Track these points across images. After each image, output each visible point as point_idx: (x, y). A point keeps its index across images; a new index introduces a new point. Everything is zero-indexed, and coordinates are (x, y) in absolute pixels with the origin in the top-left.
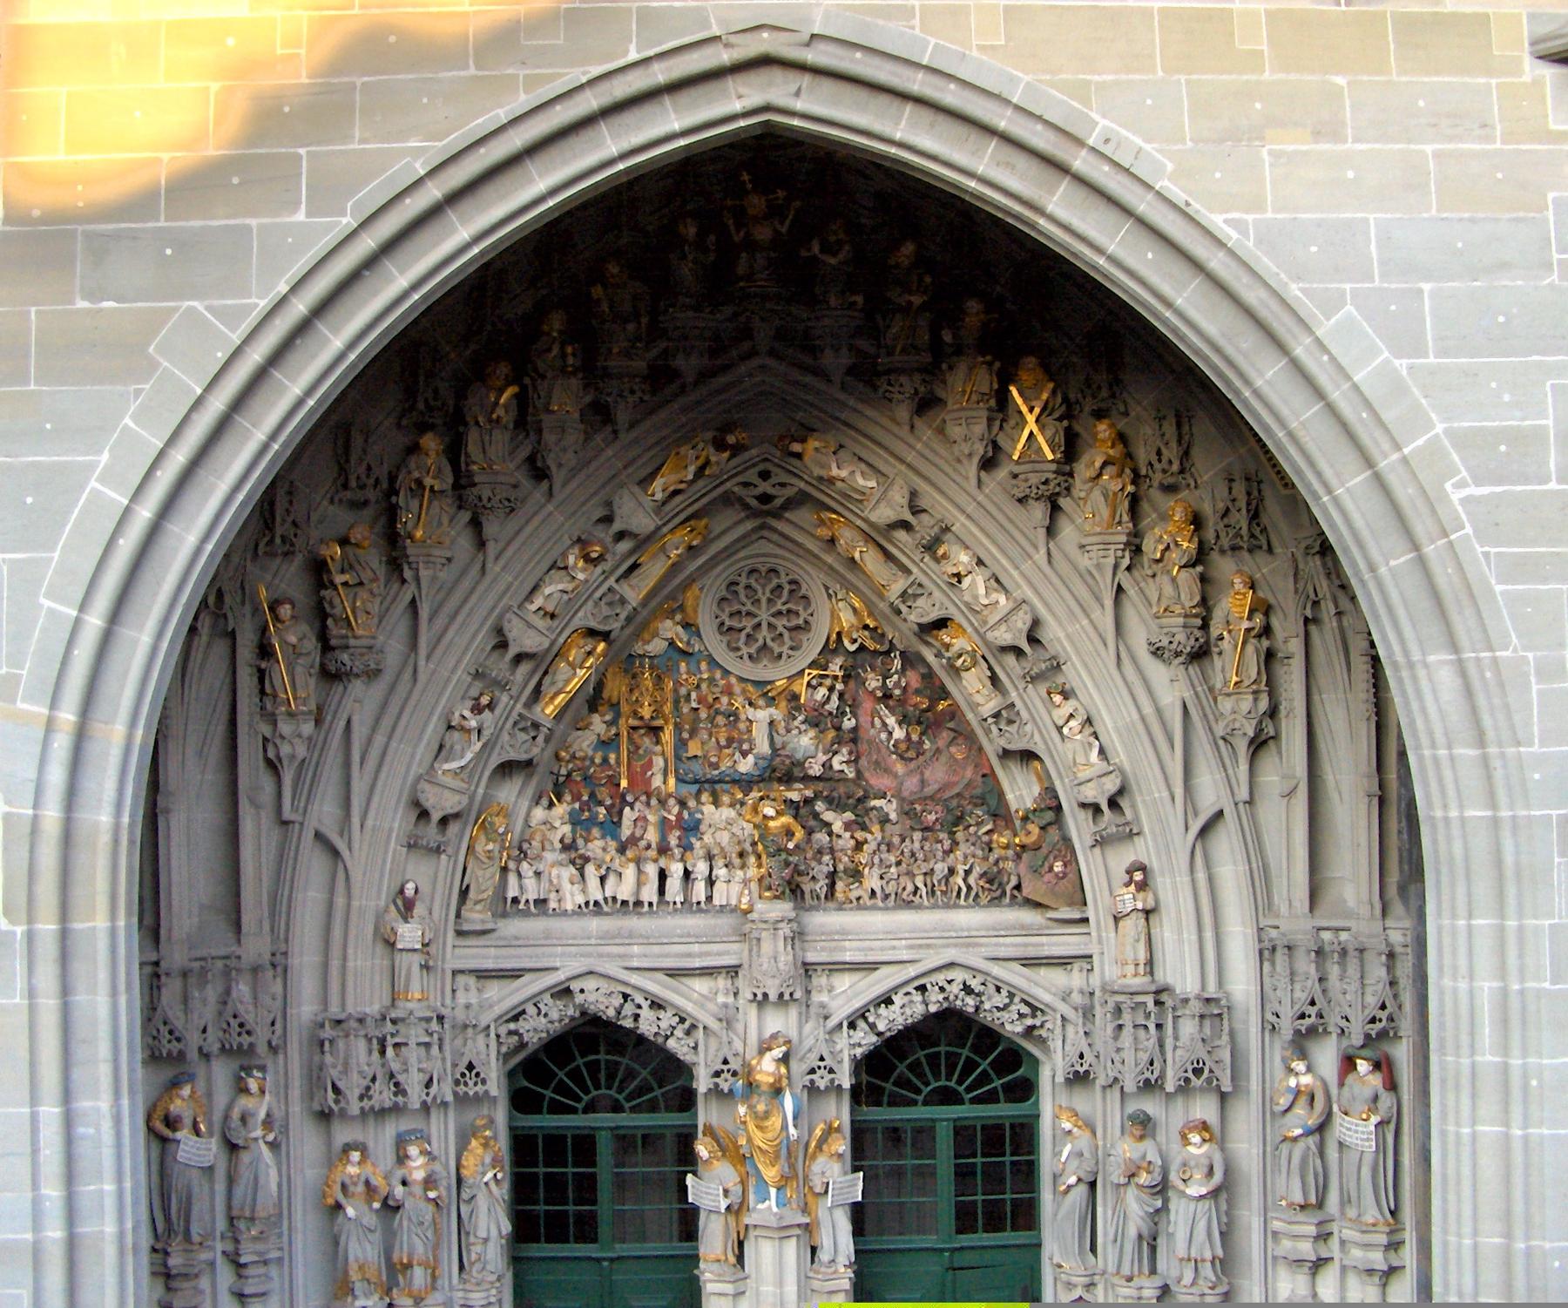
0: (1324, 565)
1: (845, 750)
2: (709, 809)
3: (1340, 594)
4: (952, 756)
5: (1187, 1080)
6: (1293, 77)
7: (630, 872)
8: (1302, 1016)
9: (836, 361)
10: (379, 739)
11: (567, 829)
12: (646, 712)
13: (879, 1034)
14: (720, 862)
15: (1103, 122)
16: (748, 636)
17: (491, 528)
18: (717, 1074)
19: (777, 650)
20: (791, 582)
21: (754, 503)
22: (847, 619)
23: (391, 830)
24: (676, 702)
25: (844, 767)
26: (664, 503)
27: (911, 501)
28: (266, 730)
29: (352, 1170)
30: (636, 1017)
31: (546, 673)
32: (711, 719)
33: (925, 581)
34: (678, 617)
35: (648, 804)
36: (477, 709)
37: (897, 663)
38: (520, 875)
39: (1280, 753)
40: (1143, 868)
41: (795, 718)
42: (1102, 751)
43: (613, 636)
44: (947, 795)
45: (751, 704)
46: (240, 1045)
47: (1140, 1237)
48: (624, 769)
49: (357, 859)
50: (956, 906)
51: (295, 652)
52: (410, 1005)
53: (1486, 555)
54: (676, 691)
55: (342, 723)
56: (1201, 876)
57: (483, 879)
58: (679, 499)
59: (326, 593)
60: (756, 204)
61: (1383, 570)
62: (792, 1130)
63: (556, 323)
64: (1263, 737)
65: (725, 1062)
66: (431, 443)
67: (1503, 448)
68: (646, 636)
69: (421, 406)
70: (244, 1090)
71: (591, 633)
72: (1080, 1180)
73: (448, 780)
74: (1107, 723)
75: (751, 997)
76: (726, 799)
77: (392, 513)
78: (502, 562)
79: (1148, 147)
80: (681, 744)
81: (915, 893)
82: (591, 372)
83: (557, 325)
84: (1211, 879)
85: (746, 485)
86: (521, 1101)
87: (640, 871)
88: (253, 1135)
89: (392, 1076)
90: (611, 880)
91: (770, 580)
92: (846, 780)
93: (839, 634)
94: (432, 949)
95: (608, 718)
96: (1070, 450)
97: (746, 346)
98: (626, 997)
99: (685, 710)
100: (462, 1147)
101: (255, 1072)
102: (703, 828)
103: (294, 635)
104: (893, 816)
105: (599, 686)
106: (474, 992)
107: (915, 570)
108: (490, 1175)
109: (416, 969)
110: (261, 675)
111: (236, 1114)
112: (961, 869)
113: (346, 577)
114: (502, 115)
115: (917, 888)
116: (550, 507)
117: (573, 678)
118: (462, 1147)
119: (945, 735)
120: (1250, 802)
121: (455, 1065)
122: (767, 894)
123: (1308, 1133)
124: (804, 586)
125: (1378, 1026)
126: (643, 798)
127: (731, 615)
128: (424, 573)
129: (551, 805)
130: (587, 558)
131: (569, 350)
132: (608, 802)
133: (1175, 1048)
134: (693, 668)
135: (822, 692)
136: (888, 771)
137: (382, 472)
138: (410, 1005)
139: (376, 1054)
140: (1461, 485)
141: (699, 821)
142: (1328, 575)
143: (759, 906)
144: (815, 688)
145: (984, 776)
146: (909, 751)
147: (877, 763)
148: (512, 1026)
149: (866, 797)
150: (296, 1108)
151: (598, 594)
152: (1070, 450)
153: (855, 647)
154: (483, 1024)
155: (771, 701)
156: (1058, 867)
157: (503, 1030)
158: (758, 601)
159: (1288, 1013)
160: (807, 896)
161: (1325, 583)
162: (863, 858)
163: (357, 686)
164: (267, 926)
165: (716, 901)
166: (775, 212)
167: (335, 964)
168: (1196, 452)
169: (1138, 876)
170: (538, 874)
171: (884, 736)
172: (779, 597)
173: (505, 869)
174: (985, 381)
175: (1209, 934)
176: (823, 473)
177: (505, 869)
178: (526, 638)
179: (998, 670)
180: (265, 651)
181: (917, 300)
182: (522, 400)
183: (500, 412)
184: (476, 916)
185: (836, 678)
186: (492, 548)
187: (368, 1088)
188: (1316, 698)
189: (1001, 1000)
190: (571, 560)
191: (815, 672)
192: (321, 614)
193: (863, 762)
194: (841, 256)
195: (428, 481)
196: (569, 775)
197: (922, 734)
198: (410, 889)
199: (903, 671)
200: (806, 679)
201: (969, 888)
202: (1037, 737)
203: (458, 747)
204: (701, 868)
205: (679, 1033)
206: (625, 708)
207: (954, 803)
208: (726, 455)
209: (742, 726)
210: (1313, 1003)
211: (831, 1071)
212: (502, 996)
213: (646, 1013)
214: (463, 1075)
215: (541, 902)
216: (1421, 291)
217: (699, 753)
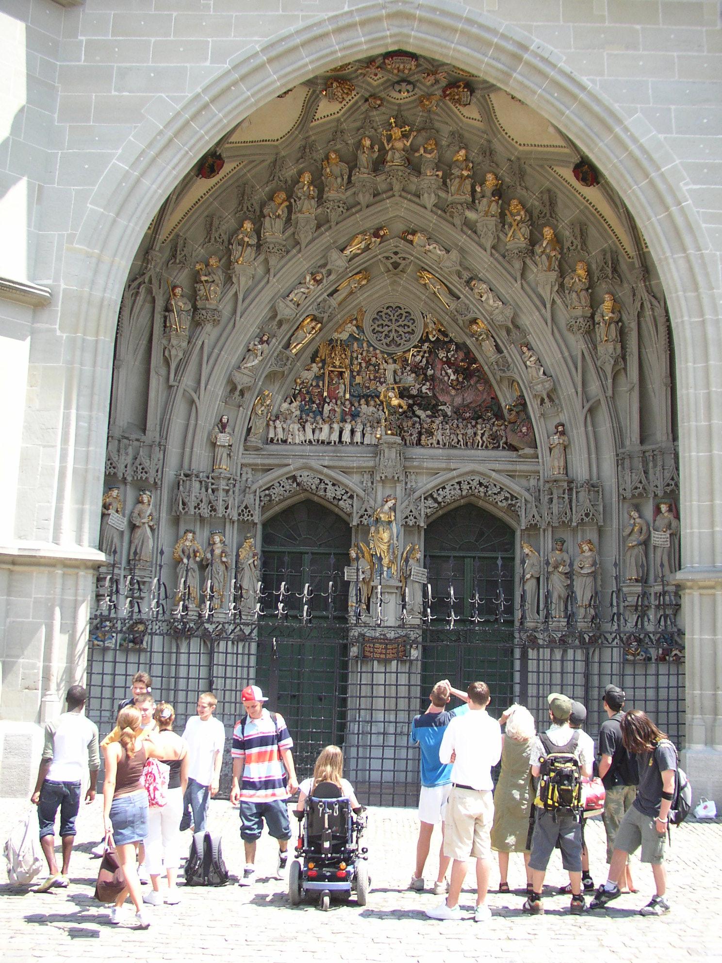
0: (645, 286)
2: (364, 407)
3: (653, 300)
4: (477, 388)
5: (582, 519)
6: (617, 25)
8: (636, 488)
9: (429, 200)
10: (216, 351)
11: (298, 413)
13: (439, 503)
14: (368, 425)
15: (537, 40)
17: (273, 261)
18: (362, 517)
19: (399, 342)
21: (390, 267)
22: (431, 325)
23: (218, 395)
26: (350, 260)
27: (461, 262)
28: (165, 342)
29: (188, 543)
30: (325, 489)
31: (293, 334)
32: (367, 367)
33: (467, 302)
34: (354, 322)
36: (262, 342)
37: (453, 347)
38: (275, 427)
39: (626, 374)
40: (563, 425)
42: (544, 373)
43: (325, 320)
44: (473, 405)
45: (386, 362)
46: (141, 478)
47: (560, 597)
48: (326, 388)
49: (202, 405)
50: (477, 449)
51: (180, 311)
52: (220, 471)
53: (698, 212)
54: (351, 356)
55: (201, 343)
56: (590, 428)
57: (259, 426)
58: (357, 259)
59: (197, 286)
60: (397, 133)
61: (653, 219)
62: (395, 542)
63: (306, 178)
64: (618, 368)
65: (366, 511)
66: (248, 225)
67: (705, 171)
68: (340, 330)
69: (245, 209)
70: (139, 502)
71: (315, 319)
72: (532, 576)
73: (246, 371)
74: (548, 361)
75: (379, 479)
76: (372, 403)
77: (229, 252)
78: (277, 277)
79: (556, 51)
80: (353, 377)
82: (320, 199)
83: (307, 179)
84: (595, 433)
85: (387, 258)
86: (267, 539)
87: (331, 428)
88: (143, 521)
89: (210, 502)
90: (317, 432)
94: (233, 448)
95: (320, 365)
96: (533, 241)
97: (390, 193)
98: (321, 480)
99: (356, 362)
100: (240, 546)
101: (147, 493)
102: (361, 414)
103: (180, 304)
104: (449, 414)
105: (316, 352)
106: (250, 475)
107: (462, 296)
108: (251, 561)
109: (225, 455)
110: (165, 317)
111: (136, 511)
112: (480, 432)
113: (206, 278)
114: (292, 29)
115: (459, 441)
116: (300, 255)
117: (306, 336)
118: (240, 546)
119: (475, 379)
120: (613, 397)
121: (239, 507)
122: (389, 432)
123: (640, 544)
125: (670, 488)
126: (334, 401)
127: (378, 326)
128: (243, 280)
129: (292, 402)
130: (315, 279)
131: (312, 188)
132: (318, 402)
133: (577, 506)
135: (419, 358)
136: (448, 393)
137: (225, 237)
138: (220, 471)
139: (203, 489)
140: (686, 184)
141: (359, 412)
142: (647, 291)
143: (384, 437)
145: (492, 398)
146: (458, 387)
147: (442, 390)
148: (267, 492)
149: (437, 405)
150: (164, 515)
151: (319, 300)
152: (533, 241)
154: (254, 488)
155: (395, 362)
156: (524, 430)
157: (263, 494)
159: (629, 487)
160: (408, 442)
161: (646, 294)
162: (435, 426)
163: (208, 327)
164: (158, 429)
165: (365, 443)
166: (405, 136)
167: (188, 450)
168: (589, 243)
169: (560, 429)
170: (283, 429)
171: (446, 378)
173: (268, 425)
174: (494, 209)
175: (593, 456)
176: (423, 249)
177: (268, 425)
178: (286, 310)
179: (498, 341)
180: (168, 309)
181: (465, 173)
182: (290, 208)
183: (280, 212)
184: (254, 440)
185: (425, 352)
186: (272, 272)
187: (198, 505)
188: (643, 350)
189: (496, 490)
190: (308, 278)
192: (193, 297)
193: (437, 389)
194: (433, 155)
195: (246, 239)
196: (300, 390)
197: (464, 379)
198: (225, 420)
199: (456, 351)
201: (483, 442)
202: (515, 370)
203: (252, 357)
204: (359, 429)
205: (344, 497)
206: (328, 360)
207: (478, 409)
208: (379, 240)
209: (382, 371)
210: (641, 482)
211: (415, 518)
212: (264, 480)
213: (330, 487)
214: (242, 511)
215: (285, 441)
216: (670, 109)
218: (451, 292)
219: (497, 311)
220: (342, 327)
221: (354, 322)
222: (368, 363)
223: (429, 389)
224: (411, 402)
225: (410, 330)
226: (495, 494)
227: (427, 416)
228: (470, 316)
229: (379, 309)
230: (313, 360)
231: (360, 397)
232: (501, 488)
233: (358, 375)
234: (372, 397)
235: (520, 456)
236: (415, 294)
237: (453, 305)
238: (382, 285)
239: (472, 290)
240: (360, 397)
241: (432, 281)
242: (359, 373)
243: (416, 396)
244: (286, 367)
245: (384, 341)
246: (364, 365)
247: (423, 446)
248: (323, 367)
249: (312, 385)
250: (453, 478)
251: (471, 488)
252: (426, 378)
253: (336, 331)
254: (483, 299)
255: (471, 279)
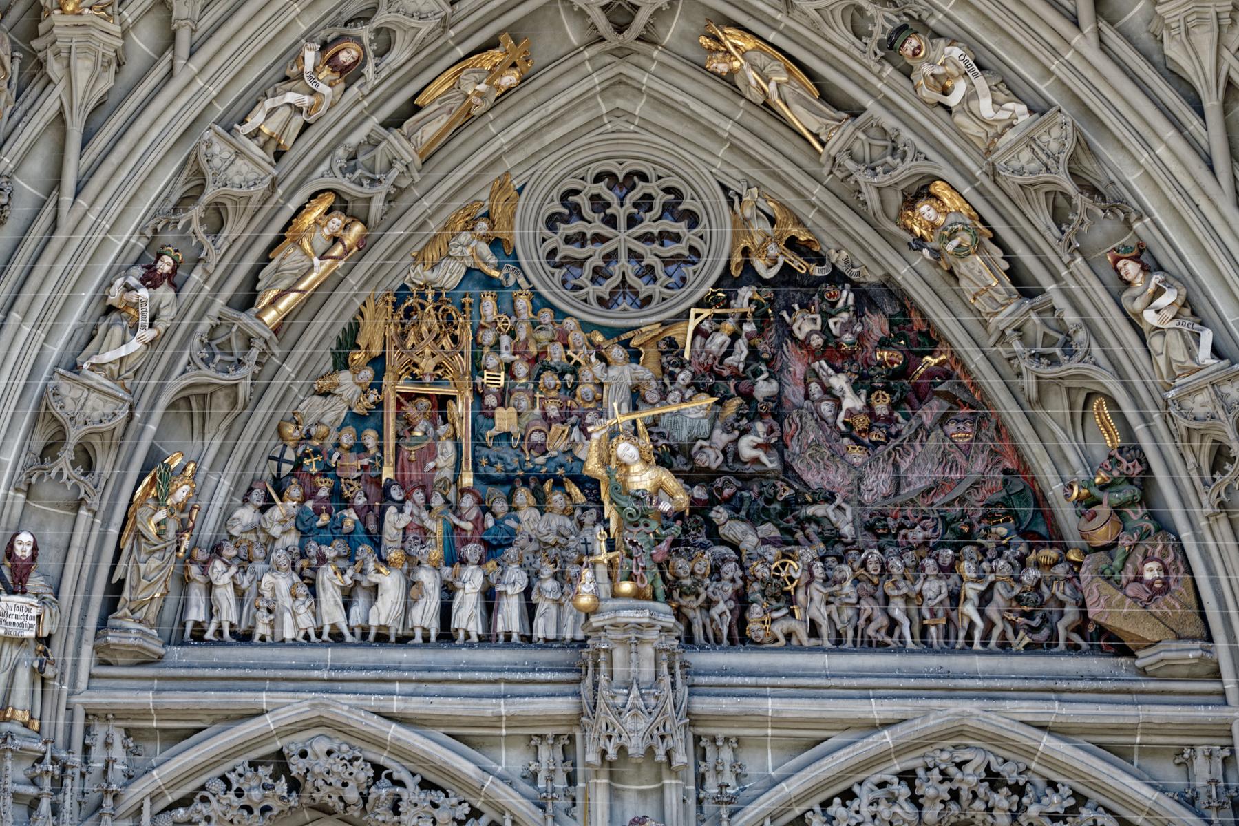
1: (760, 427)
7: (391, 583)
12: (427, 365)
16: (596, 270)
20: (667, 190)
24: (476, 359)
25: (760, 454)
33: (889, 122)
34: (483, 226)
35: (429, 509)
41: (673, 377)
45: (601, 358)
54: (477, 344)
68: (432, 255)
76: (557, 498)
80: (484, 414)
81: (890, 633)
91: (634, 187)
92: (763, 475)
93: (746, 251)
95: (367, 374)
99: (492, 361)
105: (353, 330)
107: (869, 103)
115: (893, 623)
124: (687, 192)
126: (419, 496)
127: (568, 240)
134: (506, 306)
135: (719, 340)
144: (706, 335)
153: (776, 269)
155: (635, 356)
158: (613, 217)
162: (795, 569)
172: (650, 209)
185: (743, 317)
191: (706, 312)
200: (693, 323)
206: (394, 359)
209: (586, 390)
217: (515, 430)
218: (827, 94)
219: (1010, 136)
220: (440, 244)
221: (483, 226)
222: (539, 363)
223: (765, 447)
224: (699, 492)
225: (681, 248)
226: (1054, 818)
227: (764, 541)
228: (905, 170)
229: (569, 184)
230: (341, 363)
231: (508, 482)
232: (1075, 794)
233: (501, 404)
234: (559, 484)
235: (1143, 671)
236: (693, 119)
237: (840, 135)
238: (576, 91)
239: (907, 72)
240: (508, 482)
241: (761, 60)
242: (504, 398)
243: (718, 473)
244: (243, 371)
245: (592, 290)
246: (521, 369)
247: (758, 645)
248: (377, 385)
249: (338, 445)
250: (883, 758)
251: (955, 795)
252: (752, 410)
253: (418, 258)
254: (953, 100)
255: (904, 28)
